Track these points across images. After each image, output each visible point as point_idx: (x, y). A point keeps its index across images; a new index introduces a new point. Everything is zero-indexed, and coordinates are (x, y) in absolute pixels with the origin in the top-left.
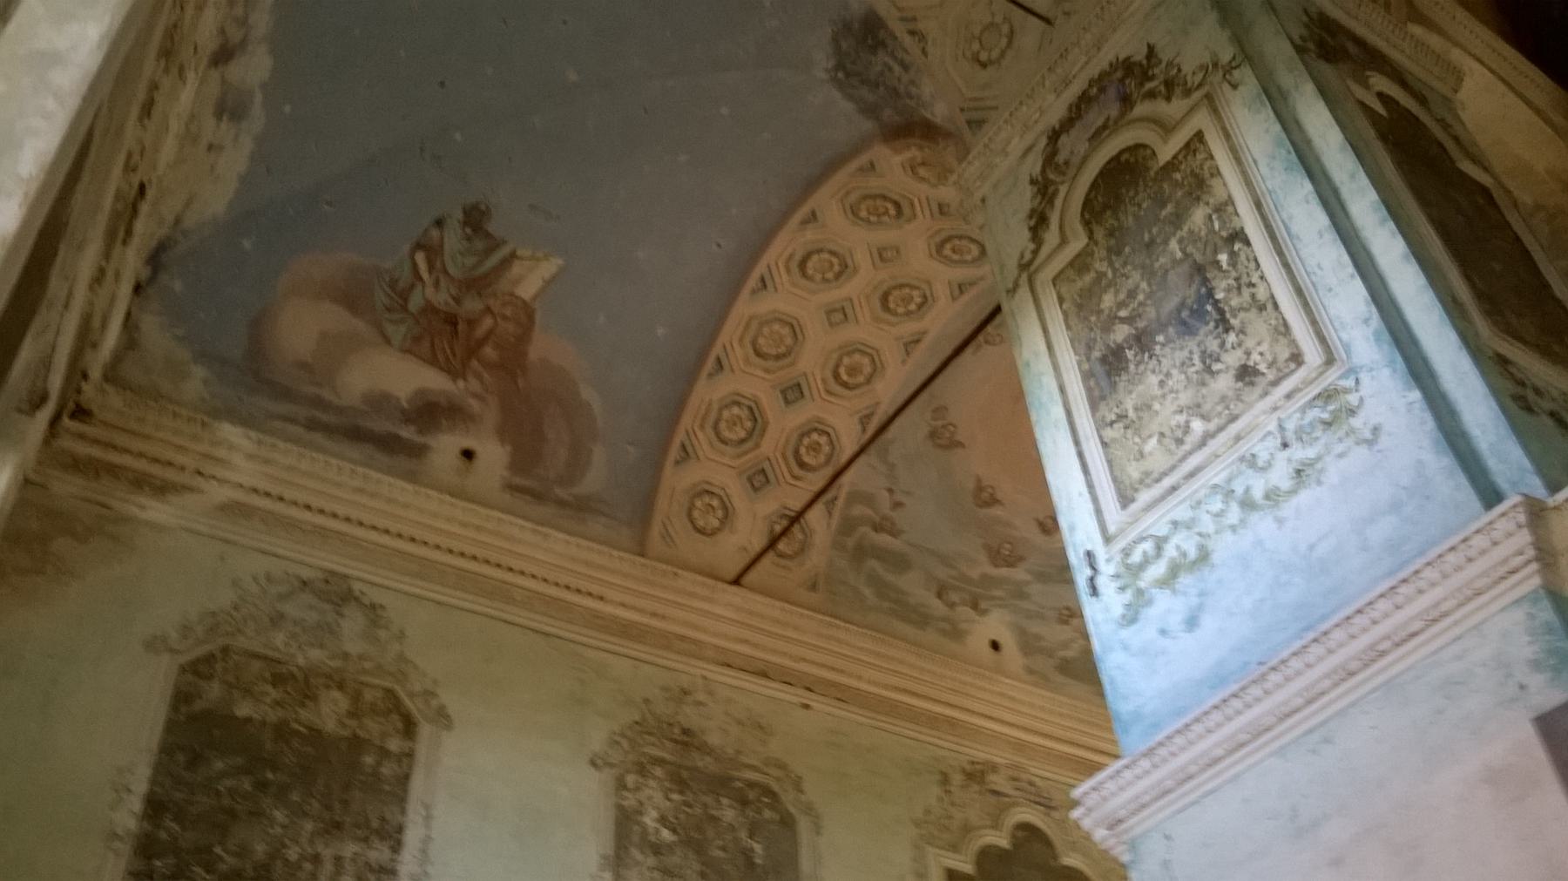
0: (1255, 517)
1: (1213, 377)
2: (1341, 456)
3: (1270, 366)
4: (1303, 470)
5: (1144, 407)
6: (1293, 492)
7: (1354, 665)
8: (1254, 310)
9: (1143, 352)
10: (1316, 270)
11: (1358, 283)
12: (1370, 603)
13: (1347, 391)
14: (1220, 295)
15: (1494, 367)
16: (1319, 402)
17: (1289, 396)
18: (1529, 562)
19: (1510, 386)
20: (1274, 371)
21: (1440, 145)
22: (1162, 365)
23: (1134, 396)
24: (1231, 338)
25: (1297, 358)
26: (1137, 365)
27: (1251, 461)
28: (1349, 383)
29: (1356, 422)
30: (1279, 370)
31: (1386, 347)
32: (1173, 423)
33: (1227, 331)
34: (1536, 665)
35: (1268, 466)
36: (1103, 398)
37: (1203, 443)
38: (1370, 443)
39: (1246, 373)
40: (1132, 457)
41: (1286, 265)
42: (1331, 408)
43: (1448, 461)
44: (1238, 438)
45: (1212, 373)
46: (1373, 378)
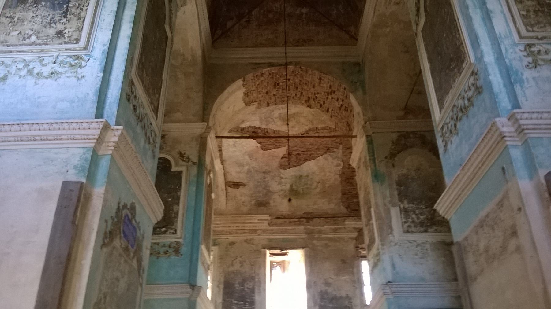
0: (29, 77)
1: (50, 27)
2: (68, 77)
3: (68, 37)
4: (54, 74)
5: (20, 20)
6: (46, 78)
7: (23, 138)
8: (77, 17)
9: (35, 4)
10: (103, 20)
11: (110, 33)
12: (43, 123)
13: (84, 60)
14: (71, 5)
15: (128, 83)
16: (74, 58)
17: (66, 49)
18: (95, 139)
19: (129, 91)
20: (69, 39)
21: (165, 15)
22: (37, 12)
23: (21, 14)
24: (64, 20)
25: (77, 41)
26: (30, 6)
27: (41, 60)
28: (86, 59)
29: (79, 71)
30: (70, 40)
31: (104, 56)
32: (27, 32)
33: (64, 17)
34: (75, 167)
35: (45, 65)
36: (10, 7)
37: (31, 45)
38: (79, 79)
39: (60, 34)
40: (5, 33)
41: (95, 12)
42: (76, 62)
43: (95, 99)
44: (42, 51)
45: (50, 26)
46: (94, 62)
